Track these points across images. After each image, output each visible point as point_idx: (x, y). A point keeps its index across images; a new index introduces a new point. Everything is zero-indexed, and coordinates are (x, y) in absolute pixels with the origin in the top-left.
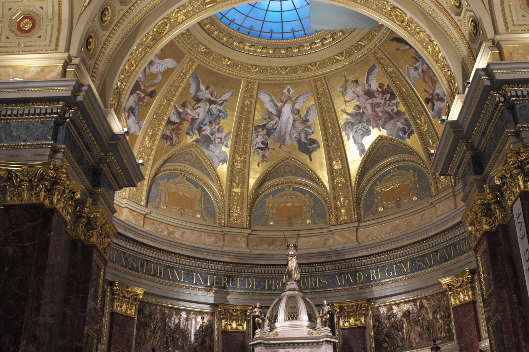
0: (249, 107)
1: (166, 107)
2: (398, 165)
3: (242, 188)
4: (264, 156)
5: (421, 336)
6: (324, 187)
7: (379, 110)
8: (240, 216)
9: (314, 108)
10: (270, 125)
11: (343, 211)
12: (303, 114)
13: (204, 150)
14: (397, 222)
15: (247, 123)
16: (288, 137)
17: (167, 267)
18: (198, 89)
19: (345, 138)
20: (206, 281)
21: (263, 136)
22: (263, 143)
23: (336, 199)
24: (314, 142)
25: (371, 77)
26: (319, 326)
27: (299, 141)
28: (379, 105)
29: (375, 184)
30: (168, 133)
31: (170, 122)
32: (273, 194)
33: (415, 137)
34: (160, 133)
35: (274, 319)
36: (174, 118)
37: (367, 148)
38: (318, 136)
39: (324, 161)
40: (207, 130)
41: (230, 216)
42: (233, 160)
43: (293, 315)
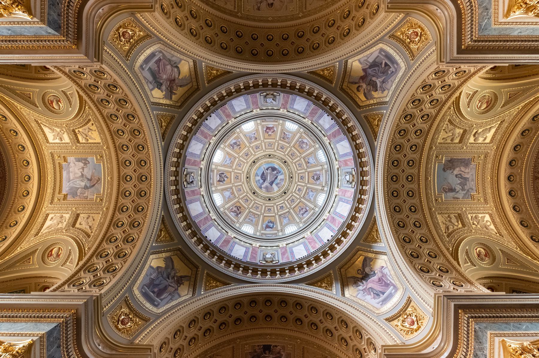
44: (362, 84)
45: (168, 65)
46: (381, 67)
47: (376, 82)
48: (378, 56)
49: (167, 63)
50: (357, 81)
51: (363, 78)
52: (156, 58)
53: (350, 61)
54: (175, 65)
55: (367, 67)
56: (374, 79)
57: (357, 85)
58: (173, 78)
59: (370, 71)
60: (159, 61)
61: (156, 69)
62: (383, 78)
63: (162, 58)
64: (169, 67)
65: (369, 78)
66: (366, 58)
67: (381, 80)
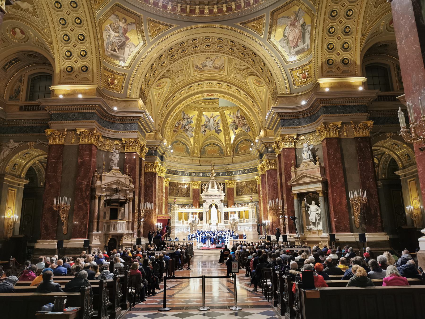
0: (200, 120)
1: (175, 122)
2: (246, 138)
3: (198, 144)
4: (204, 134)
5: (249, 191)
6: (223, 145)
7: (240, 122)
8: (197, 153)
9: (220, 120)
10: (206, 125)
11: (228, 152)
12: (217, 121)
13: (186, 133)
14: (244, 157)
15: (199, 124)
16: (212, 128)
17: (176, 171)
18: (184, 115)
19: (230, 129)
20: (187, 174)
21: (204, 128)
22: (204, 130)
23: (226, 148)
24: (220, 130)
25: (238, 113)
26: (220, 190)
27: (215, 130)
28: (240, 121)
29: (238, 144)
30: (175, 130)
31: (176, 126)
32: (207, 145)
33: (251, 132)
34: (173, 130)
35: (208, 188)
36: (177, 125)
37: (236, 133)
38: (221, 128)
39: (223, 137)
40: (187, 127)
41: (194, 154)
42: (195, 136)
43: (213, 187)
44: (124, 25)
45: (291, 40)
46: (117, 47)
47: (115, 32)
48: (123, 55)
49: (290, 42)
50: (129, 26)
51: (126, 31)
52: (296, 49)
53: (142, 44)
54: (286, 38)
55: (126, 42)
56: (117, 34)
57: (128, 22)
58: (291, 27)
59: (123, 39)
60: (296, 46)
61: (300, 41)
62: (111, 39)
63: (292, 48)
64: (291, 38)
65: (121, 33)
66: (131, 50)
67: (112, 36)
